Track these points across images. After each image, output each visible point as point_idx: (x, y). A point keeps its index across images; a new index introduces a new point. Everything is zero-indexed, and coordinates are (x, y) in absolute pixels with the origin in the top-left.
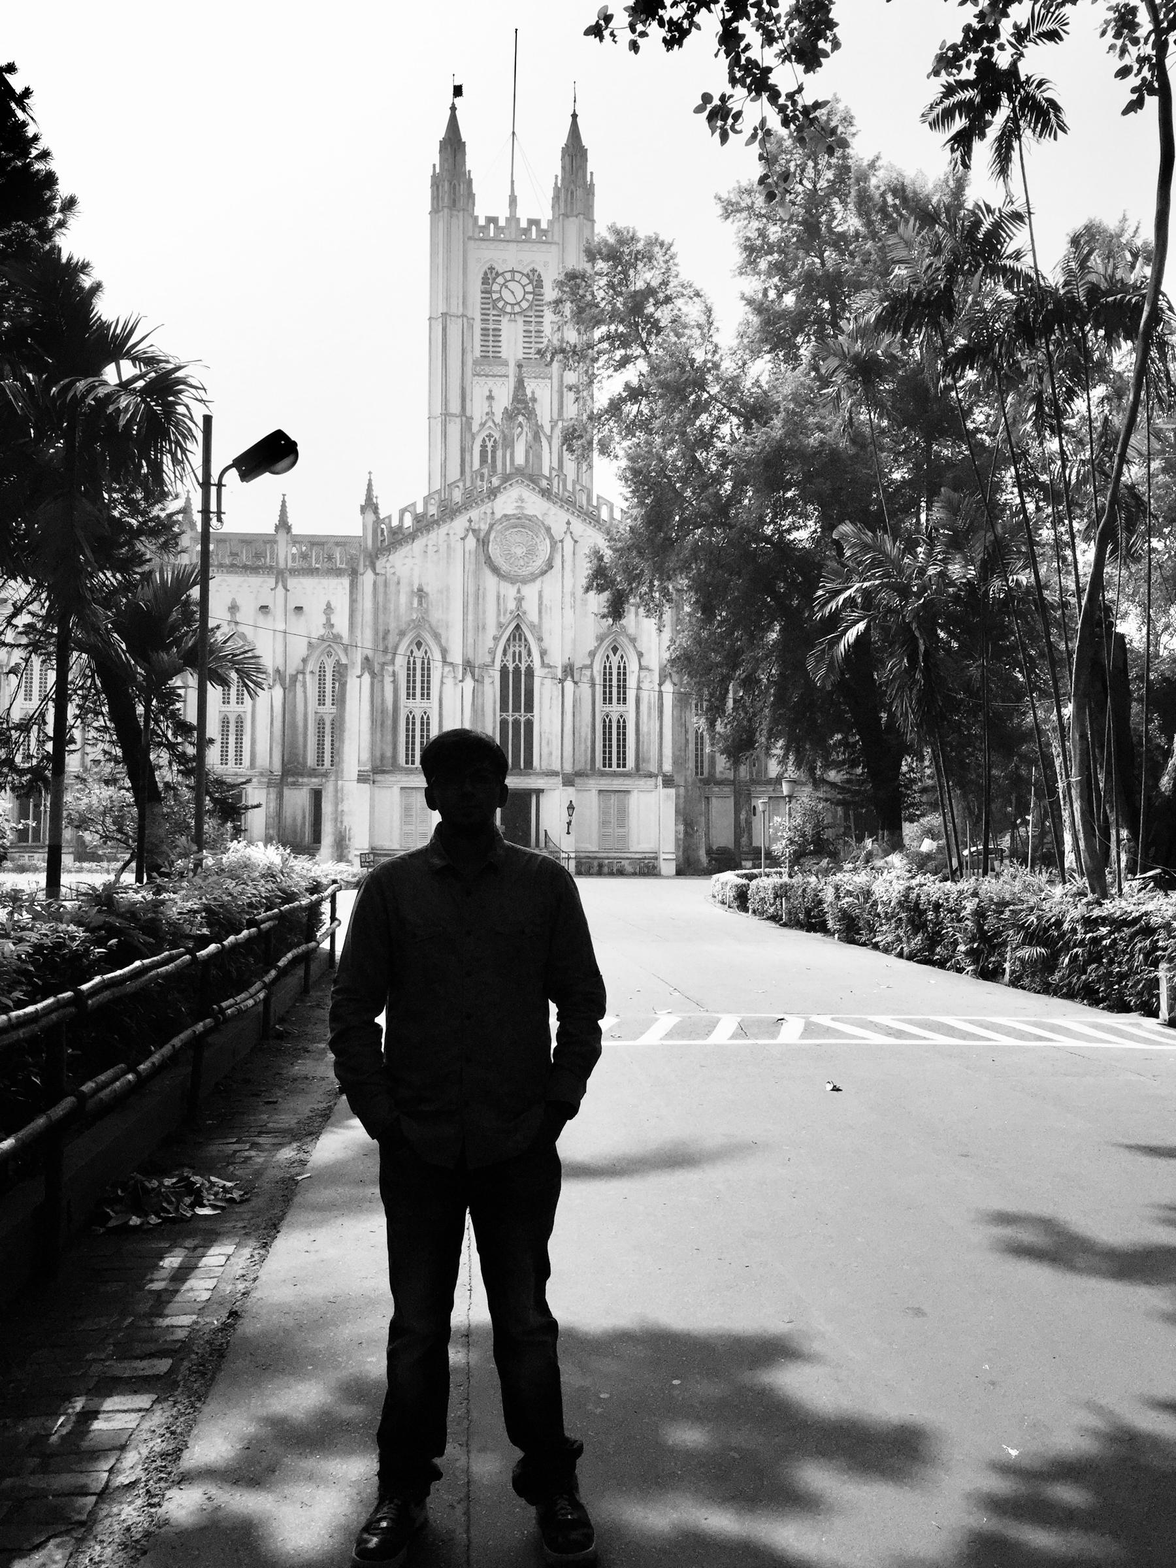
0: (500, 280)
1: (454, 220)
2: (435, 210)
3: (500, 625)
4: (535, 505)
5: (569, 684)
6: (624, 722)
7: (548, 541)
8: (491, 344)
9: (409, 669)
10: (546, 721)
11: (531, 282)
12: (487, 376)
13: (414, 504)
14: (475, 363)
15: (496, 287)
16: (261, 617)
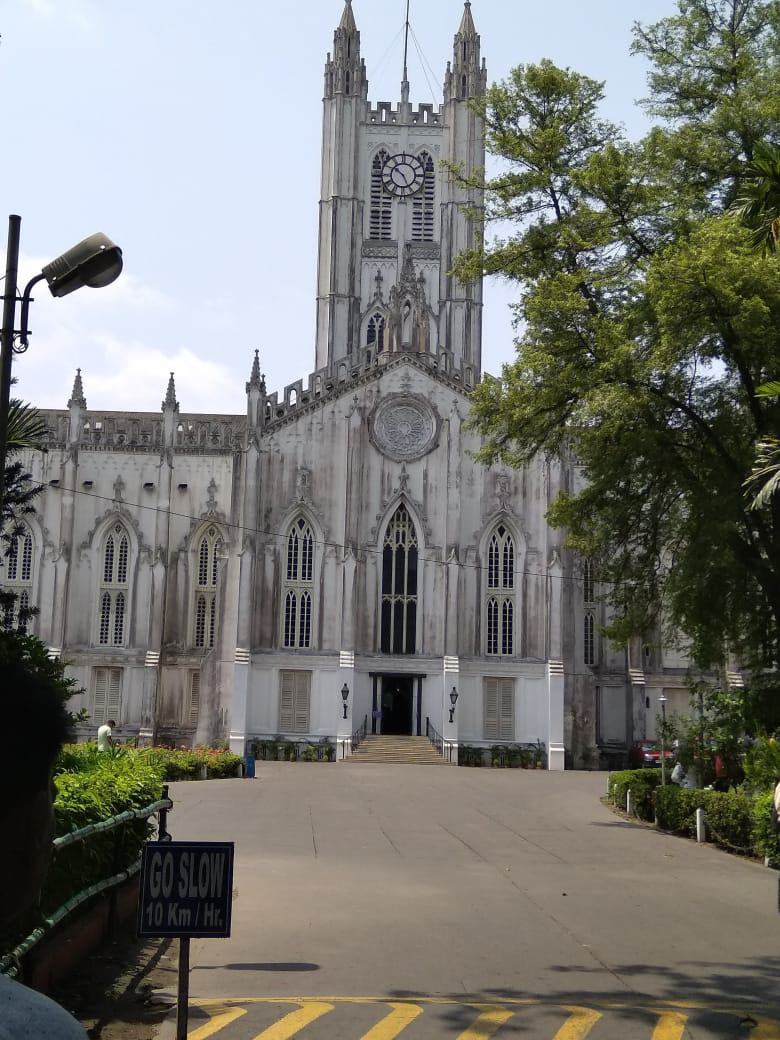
0: (391, 164)
1: (347, 106)
2: (329, 98)
3: (383, 505)
4: (422, 384)
5: (454, 568)
6: (511, 605)
7: (434, 421)
8: (380, 225)
9: (290, 548)
10: (429, 604)
11: (422, 165)
12: (376, 257)
13: (300, 383)
14: (365, 244)
15: (386, 171)
16: (145, 494)
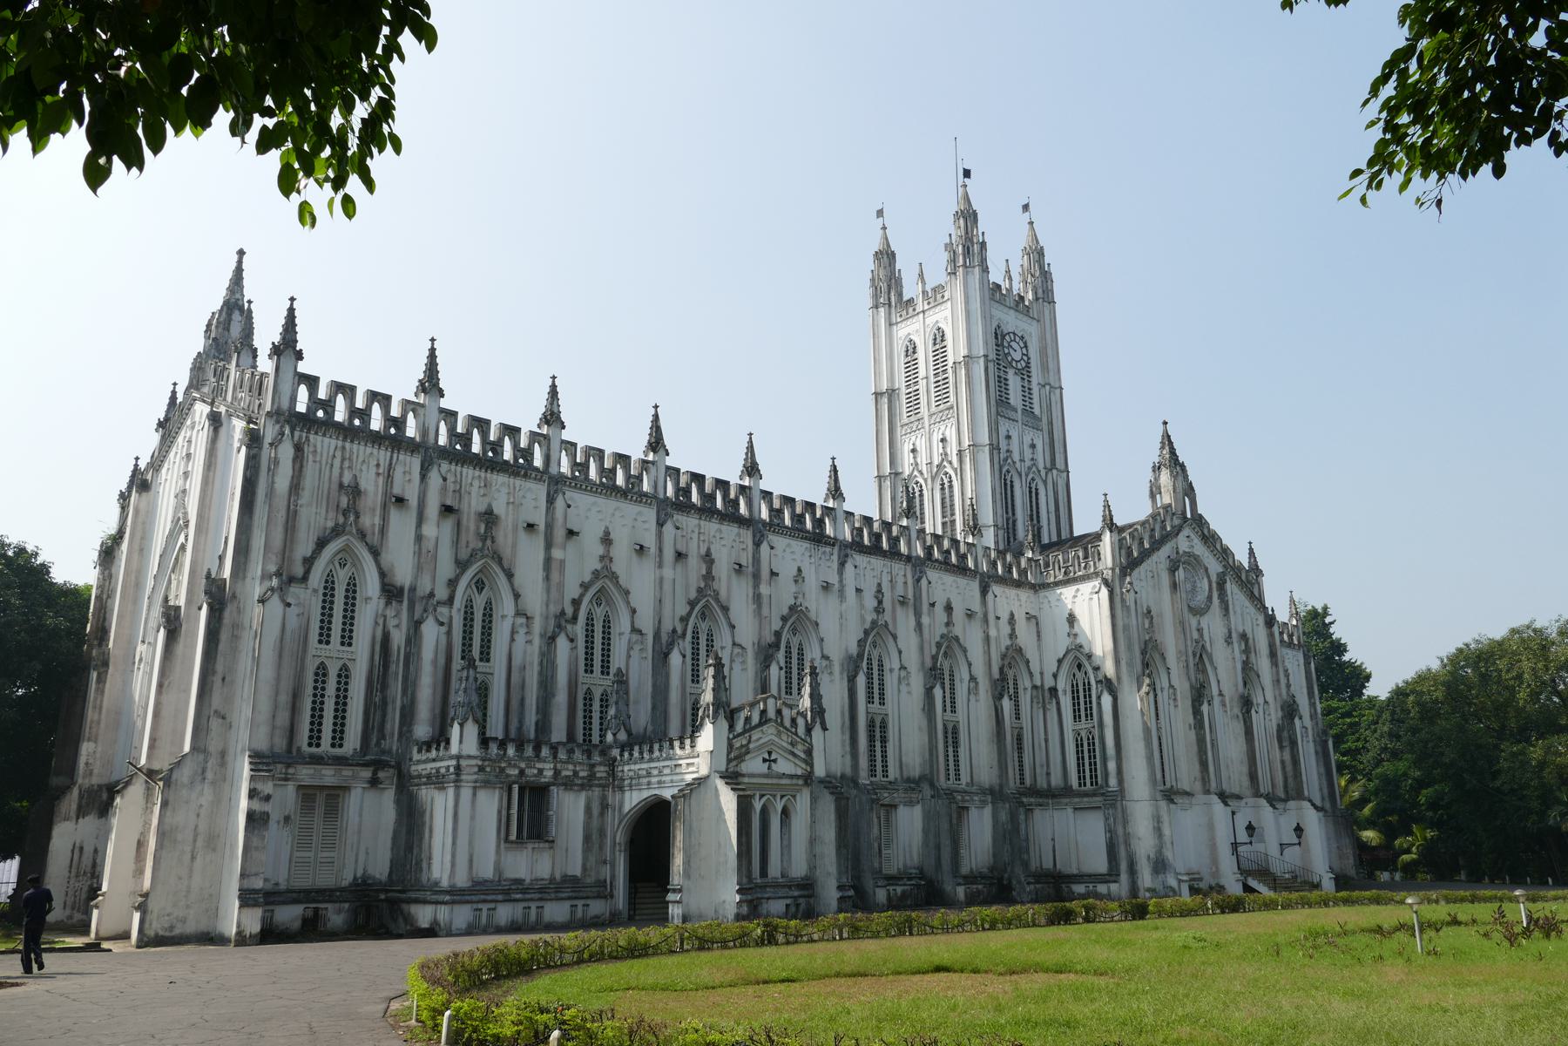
1: (970, 277)
4: (1200, 549)
7: (1206, 580)
